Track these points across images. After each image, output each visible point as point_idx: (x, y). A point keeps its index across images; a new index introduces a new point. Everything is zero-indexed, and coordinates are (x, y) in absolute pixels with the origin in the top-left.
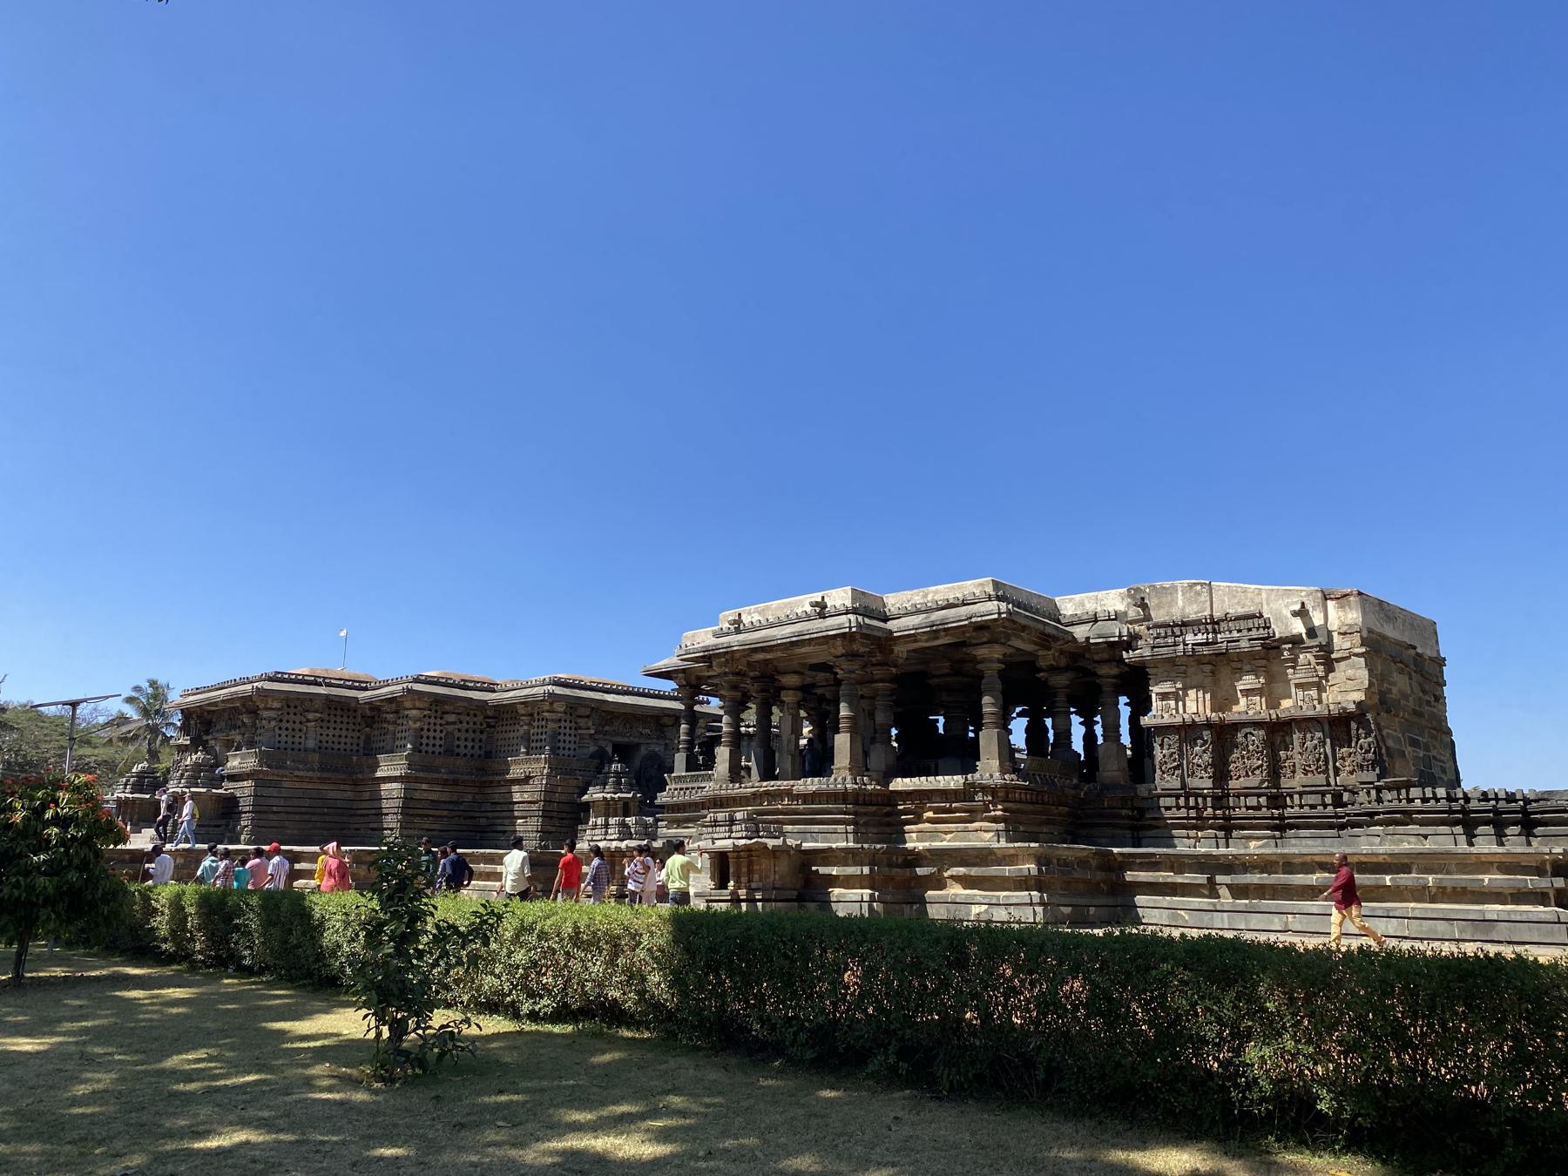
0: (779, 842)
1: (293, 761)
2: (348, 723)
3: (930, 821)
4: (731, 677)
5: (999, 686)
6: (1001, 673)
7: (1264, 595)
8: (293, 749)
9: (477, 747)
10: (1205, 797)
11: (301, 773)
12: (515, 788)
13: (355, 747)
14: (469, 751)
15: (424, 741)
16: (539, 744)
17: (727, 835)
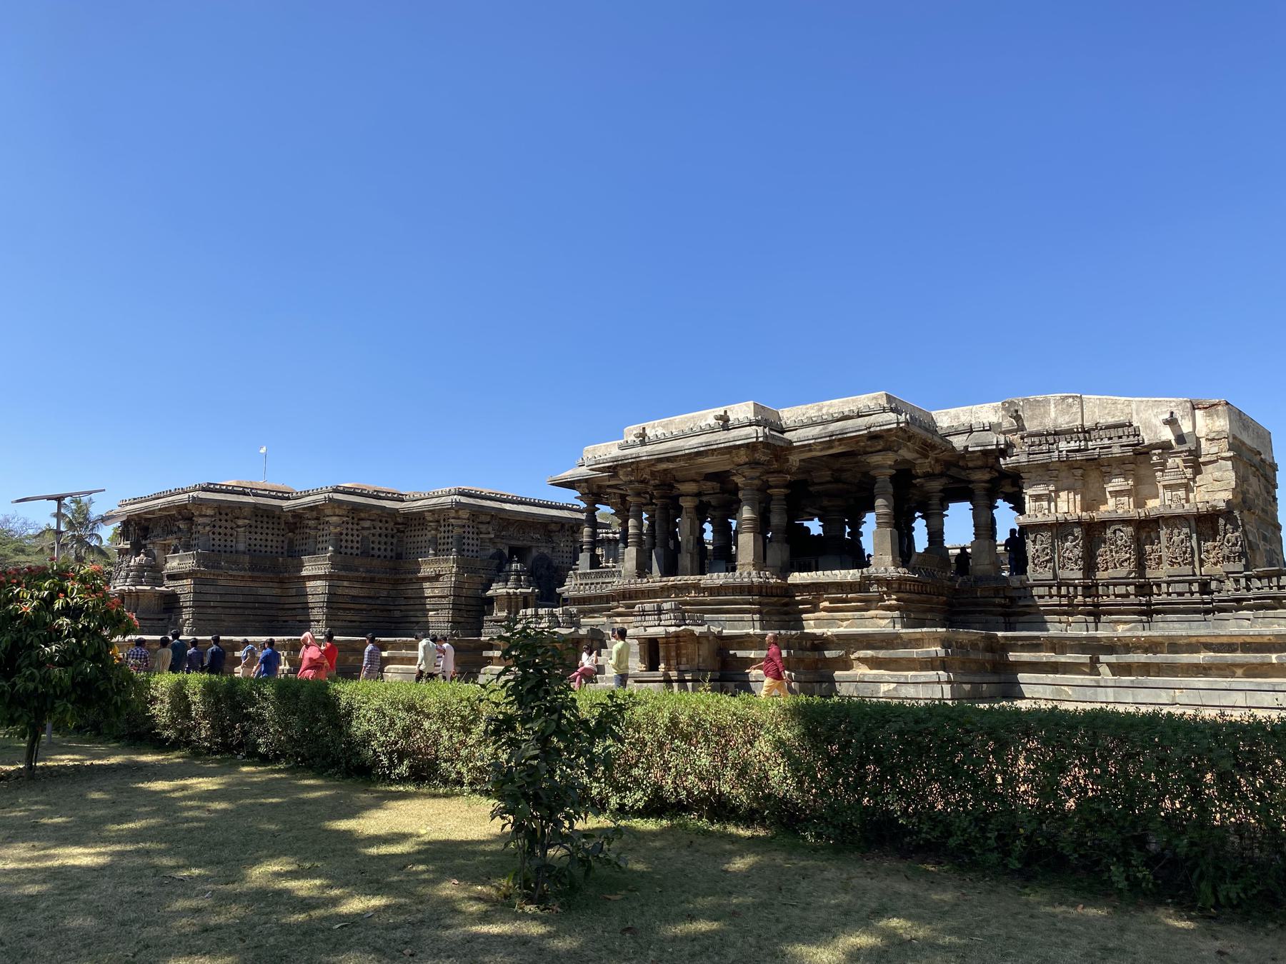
0: (704, 629)
1: (226, 562)
2: (273, 529)
3: (826, 609)
4: (637, 484)
5: (891, 490)
6: (892, 478)
7: (1134, 406)
8: (225, 552)
9: (389, 549)
10: (1075, 587)
11: (234, 573)
12: (426, 585)
13: (280, 550)
14: (382, 553)
15: (344, 544)
16: (445, 547)
17: (657, 623)
